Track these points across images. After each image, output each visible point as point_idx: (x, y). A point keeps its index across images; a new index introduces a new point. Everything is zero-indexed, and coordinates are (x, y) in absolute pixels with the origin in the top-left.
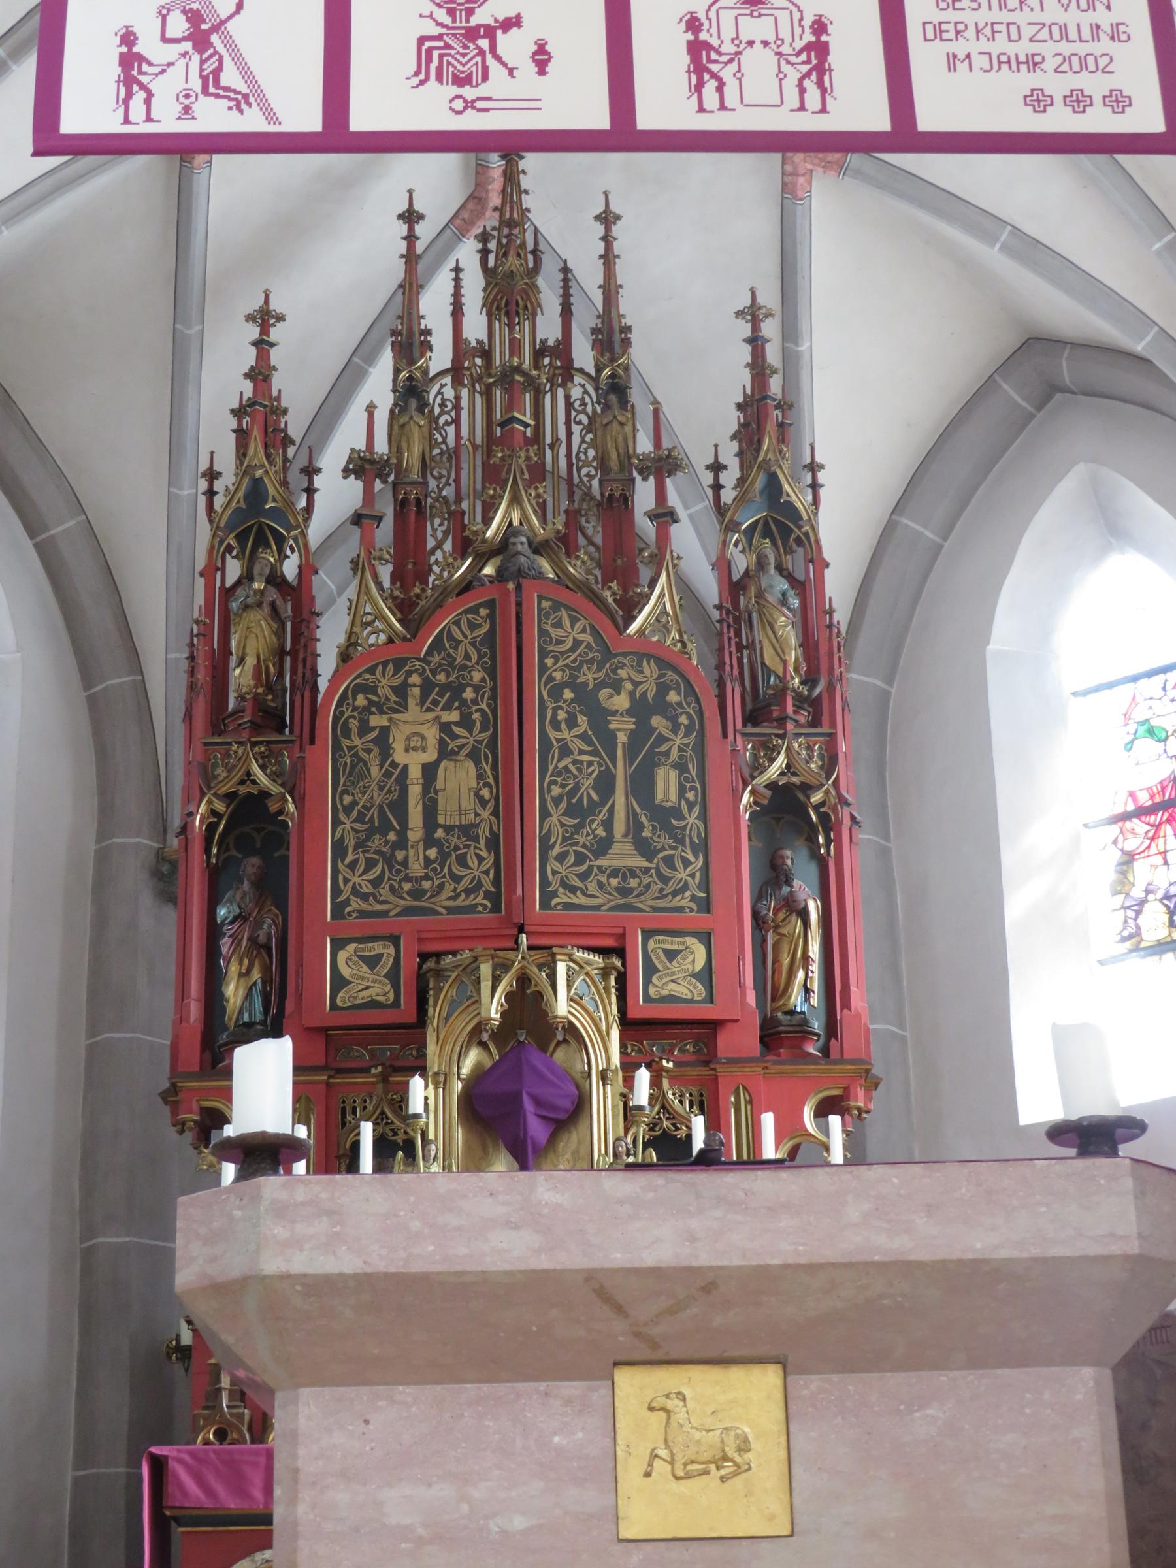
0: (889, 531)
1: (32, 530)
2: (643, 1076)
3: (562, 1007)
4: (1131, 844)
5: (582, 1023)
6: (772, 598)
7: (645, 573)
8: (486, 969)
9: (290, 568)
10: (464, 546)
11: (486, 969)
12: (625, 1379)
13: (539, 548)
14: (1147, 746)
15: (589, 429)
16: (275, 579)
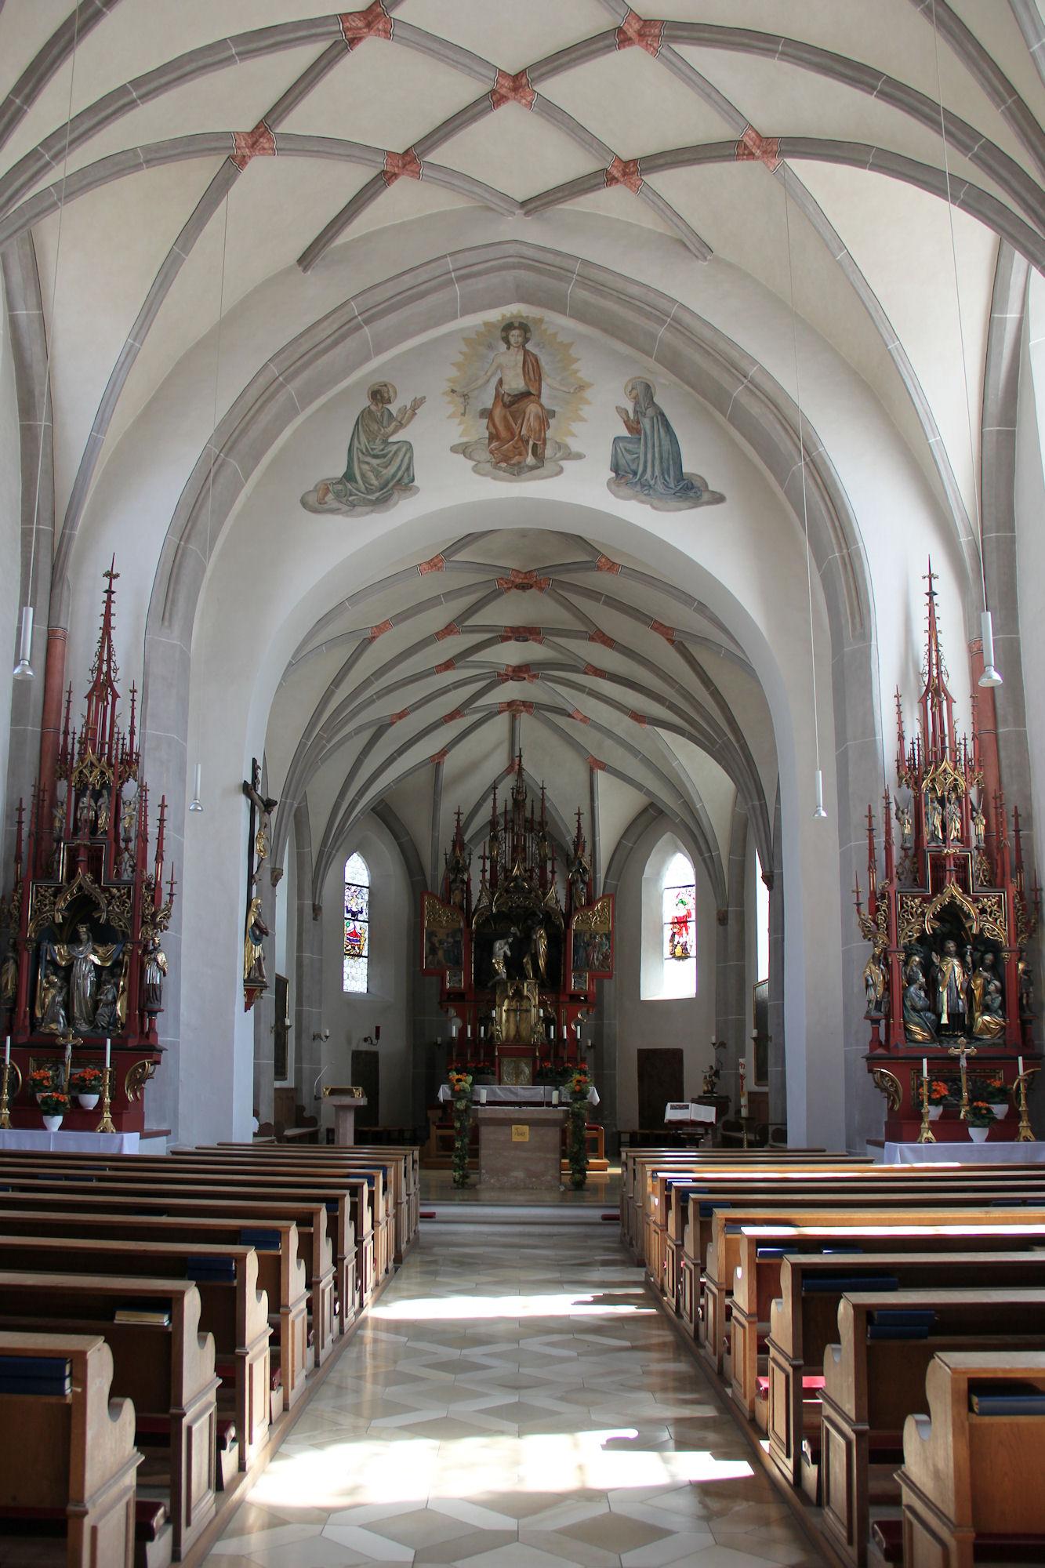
0: (619, 843)
1: (396, 837)
2: (542, 1011)
3: (525, 993)
4: (675, 930)
5: (529, 995)
6: (579, 890)
7: (549, 885)
8: (509, 984)
9: (465, 877)
10: (506, 877)
11: (509, 984)
12: (514, 1127)
13: (524, 880)
14: (681, 905)
15: (537, 845)
16: (463, 881)
